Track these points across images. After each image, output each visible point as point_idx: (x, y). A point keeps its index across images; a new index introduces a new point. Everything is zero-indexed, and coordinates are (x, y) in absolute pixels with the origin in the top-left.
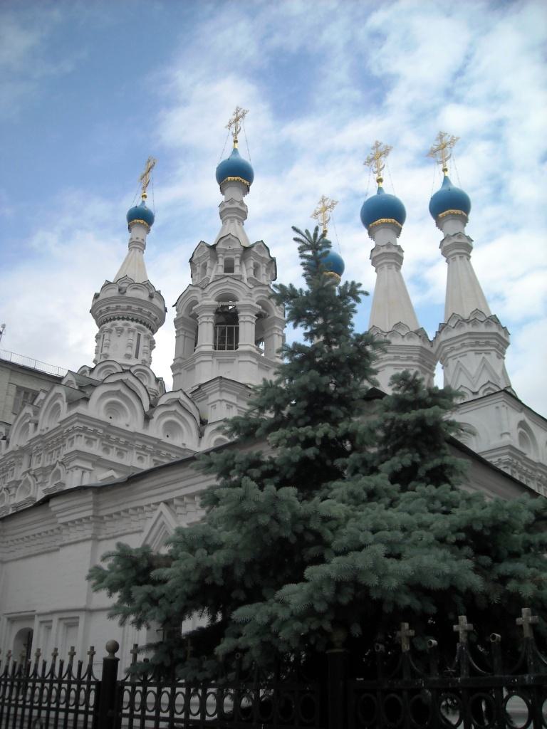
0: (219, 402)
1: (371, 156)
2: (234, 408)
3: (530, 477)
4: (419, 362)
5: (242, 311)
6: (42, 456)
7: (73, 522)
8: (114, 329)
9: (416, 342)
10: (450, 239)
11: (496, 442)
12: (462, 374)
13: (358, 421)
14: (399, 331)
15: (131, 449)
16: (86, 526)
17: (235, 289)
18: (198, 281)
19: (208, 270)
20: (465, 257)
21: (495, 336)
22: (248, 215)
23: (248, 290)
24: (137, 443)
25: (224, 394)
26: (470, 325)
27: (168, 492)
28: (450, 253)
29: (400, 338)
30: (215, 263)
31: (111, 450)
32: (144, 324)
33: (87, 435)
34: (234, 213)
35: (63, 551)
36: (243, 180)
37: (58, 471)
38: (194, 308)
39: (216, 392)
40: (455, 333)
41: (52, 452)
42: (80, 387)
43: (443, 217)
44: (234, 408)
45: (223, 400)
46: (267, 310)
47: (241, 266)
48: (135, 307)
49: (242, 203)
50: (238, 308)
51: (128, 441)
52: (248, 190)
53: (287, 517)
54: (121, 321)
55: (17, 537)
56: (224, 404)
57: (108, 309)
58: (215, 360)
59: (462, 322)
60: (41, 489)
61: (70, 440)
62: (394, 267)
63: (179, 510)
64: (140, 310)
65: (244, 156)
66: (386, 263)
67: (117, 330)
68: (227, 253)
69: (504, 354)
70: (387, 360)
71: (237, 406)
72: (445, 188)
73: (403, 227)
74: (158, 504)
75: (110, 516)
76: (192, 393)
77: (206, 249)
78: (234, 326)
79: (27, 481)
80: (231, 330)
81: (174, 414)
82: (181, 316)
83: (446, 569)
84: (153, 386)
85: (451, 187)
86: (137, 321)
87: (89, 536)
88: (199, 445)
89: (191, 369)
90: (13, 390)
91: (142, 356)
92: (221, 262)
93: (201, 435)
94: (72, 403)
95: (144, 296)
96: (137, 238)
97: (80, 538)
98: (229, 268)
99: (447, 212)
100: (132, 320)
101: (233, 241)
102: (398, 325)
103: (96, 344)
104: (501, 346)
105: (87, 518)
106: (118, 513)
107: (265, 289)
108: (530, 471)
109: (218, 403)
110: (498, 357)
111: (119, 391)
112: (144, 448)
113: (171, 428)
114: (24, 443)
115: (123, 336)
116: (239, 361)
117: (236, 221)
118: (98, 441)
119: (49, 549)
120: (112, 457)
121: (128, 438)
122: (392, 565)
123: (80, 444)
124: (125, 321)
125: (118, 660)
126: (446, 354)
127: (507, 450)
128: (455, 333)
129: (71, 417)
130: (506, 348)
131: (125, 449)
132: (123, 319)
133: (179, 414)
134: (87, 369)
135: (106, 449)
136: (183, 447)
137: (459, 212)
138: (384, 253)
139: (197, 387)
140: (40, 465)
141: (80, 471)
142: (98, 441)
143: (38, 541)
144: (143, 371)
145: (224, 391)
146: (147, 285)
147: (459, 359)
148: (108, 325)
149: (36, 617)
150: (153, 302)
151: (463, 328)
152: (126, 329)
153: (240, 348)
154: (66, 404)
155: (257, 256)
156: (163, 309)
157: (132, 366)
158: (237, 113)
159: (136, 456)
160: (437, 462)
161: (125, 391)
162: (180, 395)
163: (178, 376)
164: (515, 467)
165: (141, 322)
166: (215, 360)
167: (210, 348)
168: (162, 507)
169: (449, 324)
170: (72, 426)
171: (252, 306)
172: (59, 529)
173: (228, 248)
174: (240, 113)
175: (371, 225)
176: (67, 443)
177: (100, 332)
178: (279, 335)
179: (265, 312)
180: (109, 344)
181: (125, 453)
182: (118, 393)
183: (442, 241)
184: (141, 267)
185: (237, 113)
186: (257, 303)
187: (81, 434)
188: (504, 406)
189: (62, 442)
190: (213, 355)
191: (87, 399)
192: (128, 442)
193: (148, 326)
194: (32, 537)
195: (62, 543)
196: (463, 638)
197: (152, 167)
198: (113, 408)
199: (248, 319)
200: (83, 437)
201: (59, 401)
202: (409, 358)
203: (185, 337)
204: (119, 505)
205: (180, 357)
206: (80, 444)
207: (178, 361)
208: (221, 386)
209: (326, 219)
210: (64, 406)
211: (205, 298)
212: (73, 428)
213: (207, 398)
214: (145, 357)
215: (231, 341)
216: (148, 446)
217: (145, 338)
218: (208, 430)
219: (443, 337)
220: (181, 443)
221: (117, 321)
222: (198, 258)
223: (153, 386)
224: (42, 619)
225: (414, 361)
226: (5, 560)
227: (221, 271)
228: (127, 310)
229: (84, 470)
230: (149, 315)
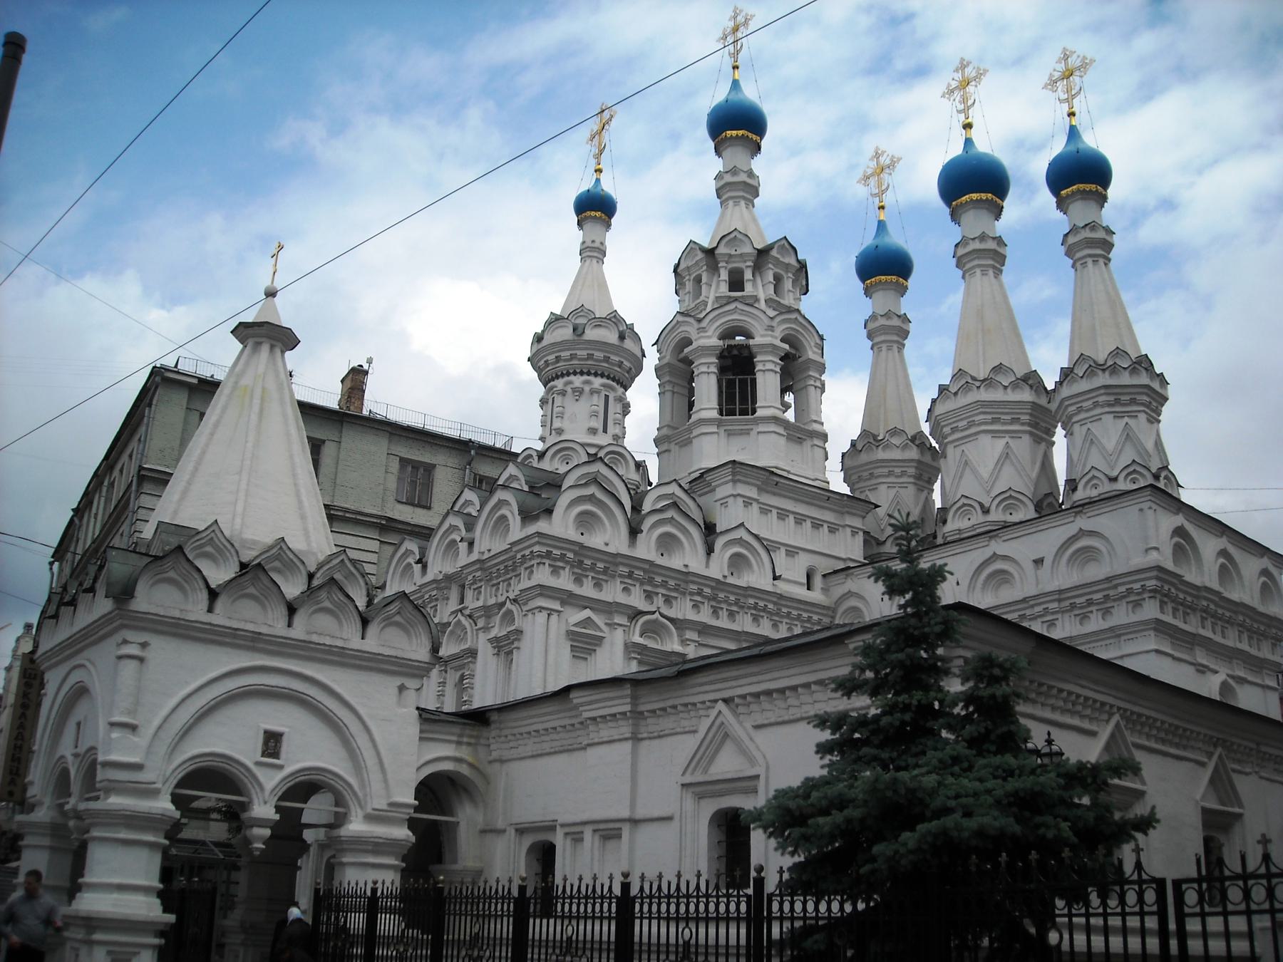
0: (732, 498)
2: (755, 505)
3: (1189, 607)
4: (1029, 425)
5: (761, 353)
6: (483, 589)
7: (603, 717)
8: (569, 389)
9: (1026, 395)
10: (1077, 232)
11: (1139, 561)
12: (1094, 450)
13: (947, 739)
14: (1000, 378)
15: (613, 577)
16: (621, 723)
17: (749, 320)
18: (689, 304)
19: (704, 287)
20: (1101, 261)
21: (1145, 390)
22: (761, 190)
23: (767, 321)
24: (621, 568)
25: (739, 485)
26: (1107, 373)
27: (730, 688)
28: (1079, 255)
29: (1001, 388)
30: (714, 274)
31: (584, 580)
32: (613, 380)
33: (551, 563)
35: (590, 751)
36: (750, 135)
37: (510, 612)
38: (686, 350)
39: (726, 483)
40: (1084, 386)
41: (499, 583)
42: (531, 487)
43: (1068, 196)
44: (755, 505)
45: (739, 495)
46: (797, 349)
47: (754, 281)
48: (599, 355)
49: (751, 174)
50: (754, 350)
51: (607, 565)
52: (759, 149)
53: (903, 791)
54: (578, 376)
55: (516, 731)
56: (740, 500)
57: (558, 359)
58: (722, 431)
59: (1095, 368)
60: (483, 638)
61: (526, 569)
62: (991, 272)
63: (741, 709)
64: (607, 359)
65: (750, 93)
66: (979, 266)
67: (574, 392)
68: (733, 260)
69: (1159, 415)
71: (759, 503)
72: (1072, 148)
73: (1005, 204)
74: (716, 701)
75: (654, 711)
76: (690, 482)
77: (700, 255)
78: (749, 377)
79: (459, 622)
80: (743, 383)
81: (670, 522)
82: (665, 361)
83: (997, 824)
84: (633, 476)
85: (1081, 146)
86: (602, 376)
87: (628, 735)
88: (707, 566)
89: (686, 445)
90: (395, 466)
91: (612, 429)
92: (724, 275)
93: (710, 550)
94: (527, 516)
95: (611, 337)
96: (593, 241)
97: (616, 737)
98: (736, 283)
99: (1074, 187)
100: (596, 375)
101: (741, 240)
102: (999, 368)
103: (541, 412)
104: (1154, 404)
105: (624, 714)
106: (664, 709)
107: (793, 316)
108: (1189, 599)
109: (731, 500)
110: (1149, 421)
111: (593, 495)
112: (630, 575)
113: (667, 543)
114: (450, 569)
115: (583, 399)
116: (759, 433)
117: (743, 203)
118: (567, 570)
119: (570, 747)
120: (587, 590)
121: (610, 563)
122: (966, 823)
123: (543, 576)
124: (585, 377)
125: (763, 878)
126: (1070, 417)
127: (1154, 573)
128: (1084, 386)
129: (528, 538)
130: (1162, 405)
131: (604, 577)
132: (582, 373)
133: (676, 521)
134: (534, 454)
135: (578, 580)
136: (684, 570)
137: (1093, 187)
138: (974, 251)
139: (697, 474)
140: (480, 603)
141: (545, 613)
142: (567, 570)
143: (555, 736)
144: (618, 454)
145: (739, 481)
146: (614, 319)
147: (1089, 425)
148: (559, 383)
149: (558, 827)
150: (625, 346)
151: (1095, 378)
152: (587, 388)
153: (760, 413)
154: (518, 518)
155: (778, 263)
156: (639, 355)
157: (601, 447)
158: (735, 18)
159: (620, 587)
160: (1005, 729)
161: (600, 495)
162: (673, 489)
163: (666, 454)
164: (1166, 595)
165: (608, 378)
166: (722, 431)
167: (714, 414)
168: (721, 706)
169: (1075, 371)
170: (530, 550)
172: (582, 723)
173: (733, 252)
174: (740, 19)
175: (954, 203)
176: (524, 574)
177: (547, 392)
178: (816, 387)
179: (793, 351)
180: (563, 414)
181: (603, 583)
182: (591, 499)
183: (1066, 235)
184: (602, 286)
185: (735, 18)
186: (782, 340)
187: (544, 561)
188: (1150, 508)
189: (513, 570)
190: (719, 424)
191: (549, 512)
192: (608, 568)
193: (618, 382)
194: (542, 732)
195: (590, 742)
196: (1003, 865)
197: (608, 122)
198: (586, 521)
199: (770, 366)
200: (547, 565)
201: (504, 511)
202: (1015, 421)
203: (674, 393)
204: (664, 700)
205: (668, 426)
206: (543, 576)
207: (665, 431)
208: (734, 474)
209: (884, 188)
210: (515, 520)
211: (702, 334)
212: (532, 552)
213: (713, 490)
214: (617, 431)
215: (744, 400)
216: (636, 572)
217: (615, 400)
218: (720, 542)
219: (1066, 391)
220: (682, 564)
221: (572, 378)
222: (688, 268)
223: (633, 476)
224: (567, 830)
225: (1023, 424)
226: (504, 758)
227: (724, 289)
228: (587, 359)
229: (550, 612)
230: (620, 364)
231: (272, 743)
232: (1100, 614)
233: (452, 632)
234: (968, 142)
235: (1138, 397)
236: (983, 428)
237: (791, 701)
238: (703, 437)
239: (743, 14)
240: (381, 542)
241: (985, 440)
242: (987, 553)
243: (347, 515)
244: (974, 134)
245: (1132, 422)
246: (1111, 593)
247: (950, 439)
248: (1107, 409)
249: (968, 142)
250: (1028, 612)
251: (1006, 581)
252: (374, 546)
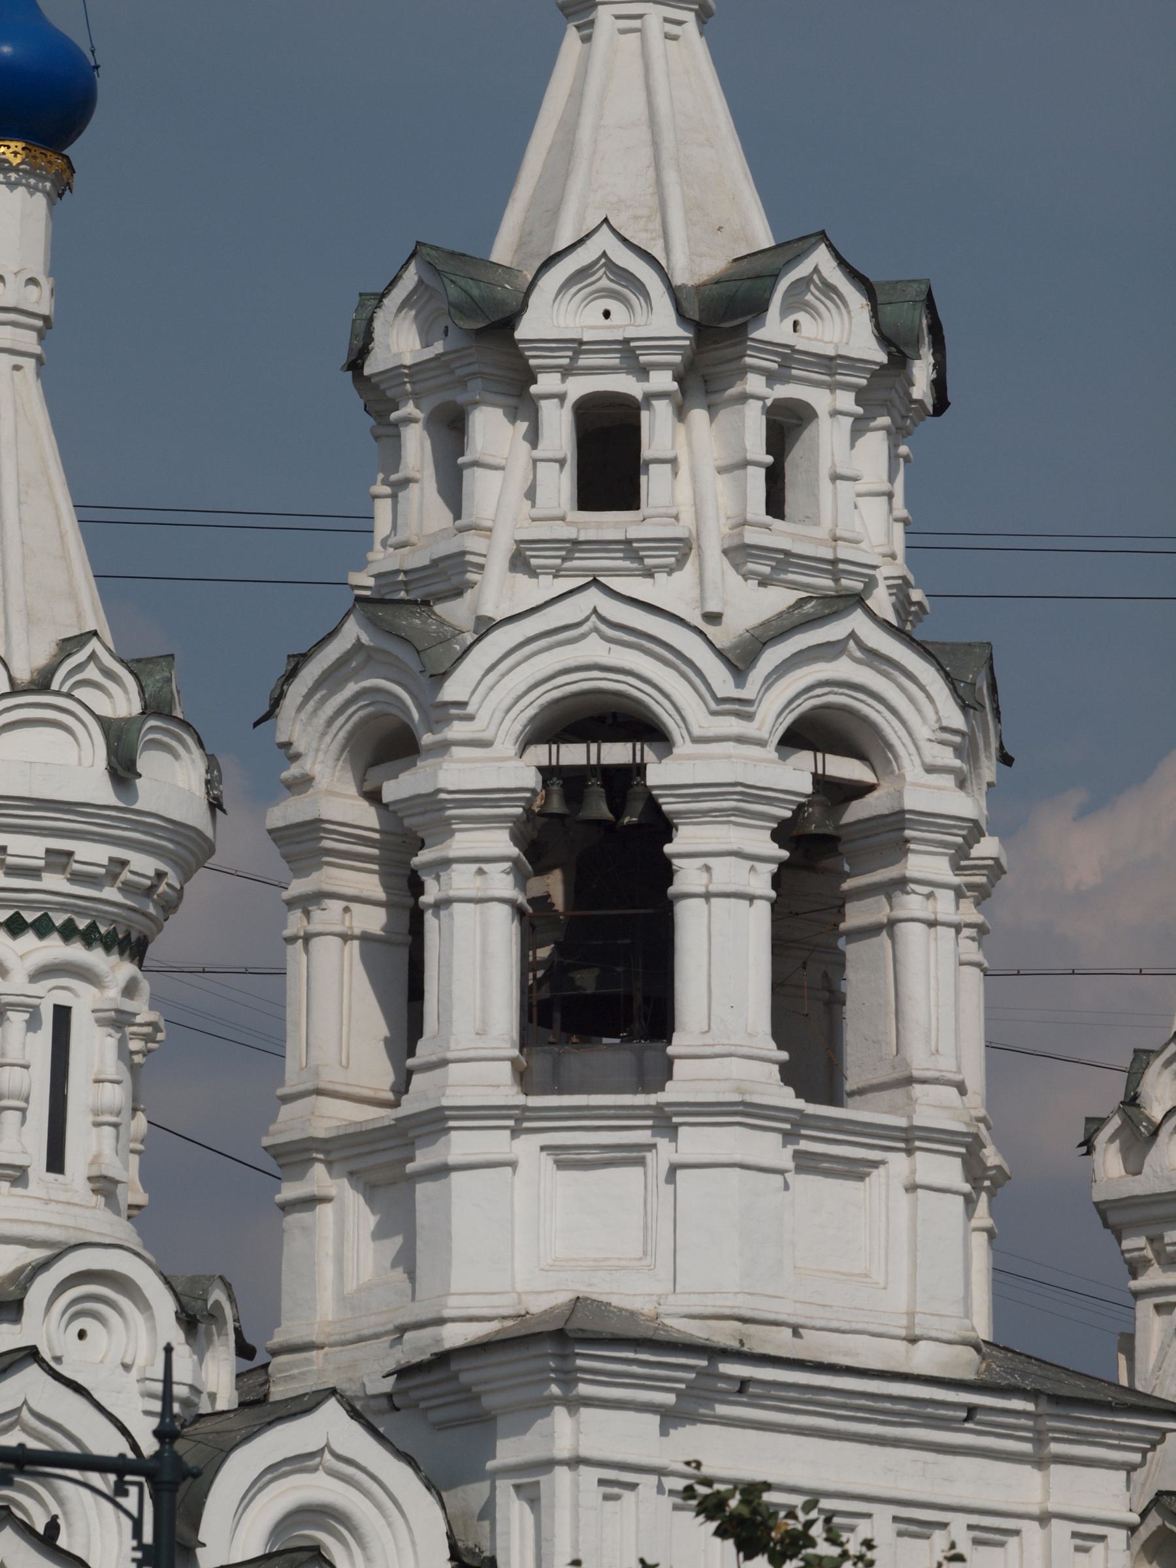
50: (669, 805)
76: (403, 1373)
86: (43, 928)
165: (68, 932)
171: (751, 793)
199: (728, 874)
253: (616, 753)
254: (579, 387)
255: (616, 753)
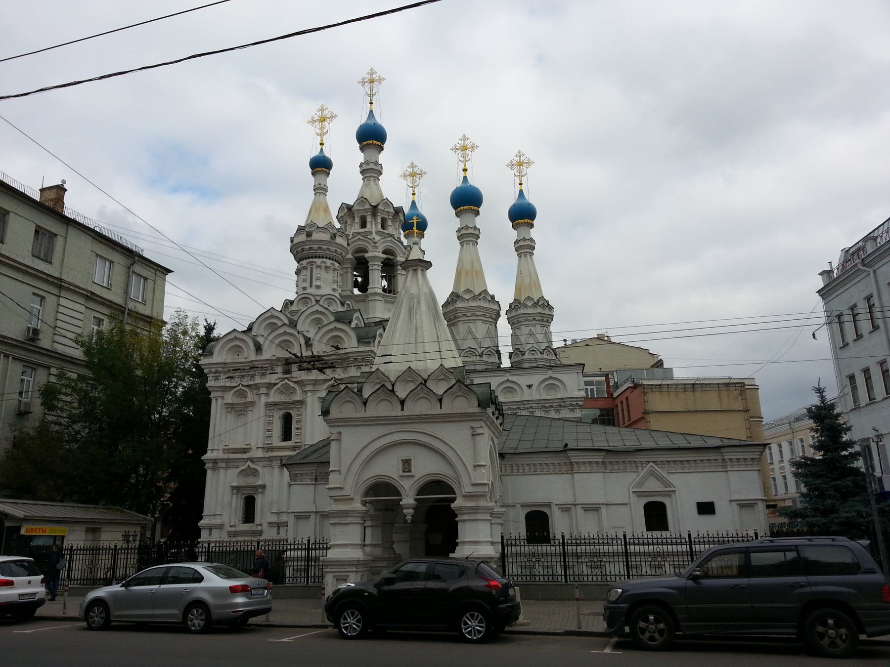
1: (459, 146)
16: (587, 465)
34: (371, 172)
40: (530, 311)
48: (339, 251)
63: (659, 466)
70: (477, 316)
75: (611, 462)
115: (331, 272)
124: (331, 261)
132: (330, 259)
148: (318, 261)
168: (651, 464)
190: (383, 296)
222: (358, 210)
227: (379, 226)
231: (407, 464)
232: (554, 411)
233: (278, 389)
234: (465, 178)
235: (536, 318)
236: (479, 318)
237: (686, 465)
238: (376, 302)
239: (378, 74)
240: (86, 307)
241: (479, 323)
242: (505, 379)
243: (71, 287)
244: (468, 174)
245: (533, 329)
246: (562, 404)
247: (460, 319)
248: (538, 322)
249: (465, 178)
250: (521, 406)
251: (513, 393)
252: (82, 309)
253: (389, 257)
254: (383, 216)
255: (389, 257)
